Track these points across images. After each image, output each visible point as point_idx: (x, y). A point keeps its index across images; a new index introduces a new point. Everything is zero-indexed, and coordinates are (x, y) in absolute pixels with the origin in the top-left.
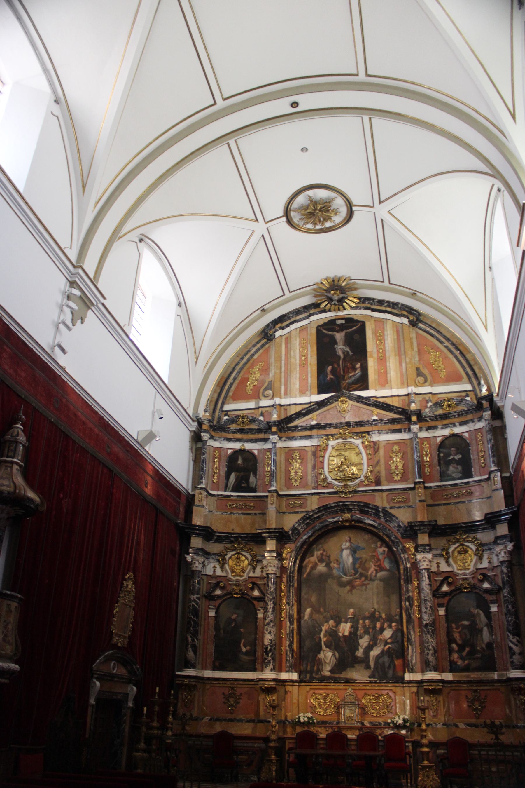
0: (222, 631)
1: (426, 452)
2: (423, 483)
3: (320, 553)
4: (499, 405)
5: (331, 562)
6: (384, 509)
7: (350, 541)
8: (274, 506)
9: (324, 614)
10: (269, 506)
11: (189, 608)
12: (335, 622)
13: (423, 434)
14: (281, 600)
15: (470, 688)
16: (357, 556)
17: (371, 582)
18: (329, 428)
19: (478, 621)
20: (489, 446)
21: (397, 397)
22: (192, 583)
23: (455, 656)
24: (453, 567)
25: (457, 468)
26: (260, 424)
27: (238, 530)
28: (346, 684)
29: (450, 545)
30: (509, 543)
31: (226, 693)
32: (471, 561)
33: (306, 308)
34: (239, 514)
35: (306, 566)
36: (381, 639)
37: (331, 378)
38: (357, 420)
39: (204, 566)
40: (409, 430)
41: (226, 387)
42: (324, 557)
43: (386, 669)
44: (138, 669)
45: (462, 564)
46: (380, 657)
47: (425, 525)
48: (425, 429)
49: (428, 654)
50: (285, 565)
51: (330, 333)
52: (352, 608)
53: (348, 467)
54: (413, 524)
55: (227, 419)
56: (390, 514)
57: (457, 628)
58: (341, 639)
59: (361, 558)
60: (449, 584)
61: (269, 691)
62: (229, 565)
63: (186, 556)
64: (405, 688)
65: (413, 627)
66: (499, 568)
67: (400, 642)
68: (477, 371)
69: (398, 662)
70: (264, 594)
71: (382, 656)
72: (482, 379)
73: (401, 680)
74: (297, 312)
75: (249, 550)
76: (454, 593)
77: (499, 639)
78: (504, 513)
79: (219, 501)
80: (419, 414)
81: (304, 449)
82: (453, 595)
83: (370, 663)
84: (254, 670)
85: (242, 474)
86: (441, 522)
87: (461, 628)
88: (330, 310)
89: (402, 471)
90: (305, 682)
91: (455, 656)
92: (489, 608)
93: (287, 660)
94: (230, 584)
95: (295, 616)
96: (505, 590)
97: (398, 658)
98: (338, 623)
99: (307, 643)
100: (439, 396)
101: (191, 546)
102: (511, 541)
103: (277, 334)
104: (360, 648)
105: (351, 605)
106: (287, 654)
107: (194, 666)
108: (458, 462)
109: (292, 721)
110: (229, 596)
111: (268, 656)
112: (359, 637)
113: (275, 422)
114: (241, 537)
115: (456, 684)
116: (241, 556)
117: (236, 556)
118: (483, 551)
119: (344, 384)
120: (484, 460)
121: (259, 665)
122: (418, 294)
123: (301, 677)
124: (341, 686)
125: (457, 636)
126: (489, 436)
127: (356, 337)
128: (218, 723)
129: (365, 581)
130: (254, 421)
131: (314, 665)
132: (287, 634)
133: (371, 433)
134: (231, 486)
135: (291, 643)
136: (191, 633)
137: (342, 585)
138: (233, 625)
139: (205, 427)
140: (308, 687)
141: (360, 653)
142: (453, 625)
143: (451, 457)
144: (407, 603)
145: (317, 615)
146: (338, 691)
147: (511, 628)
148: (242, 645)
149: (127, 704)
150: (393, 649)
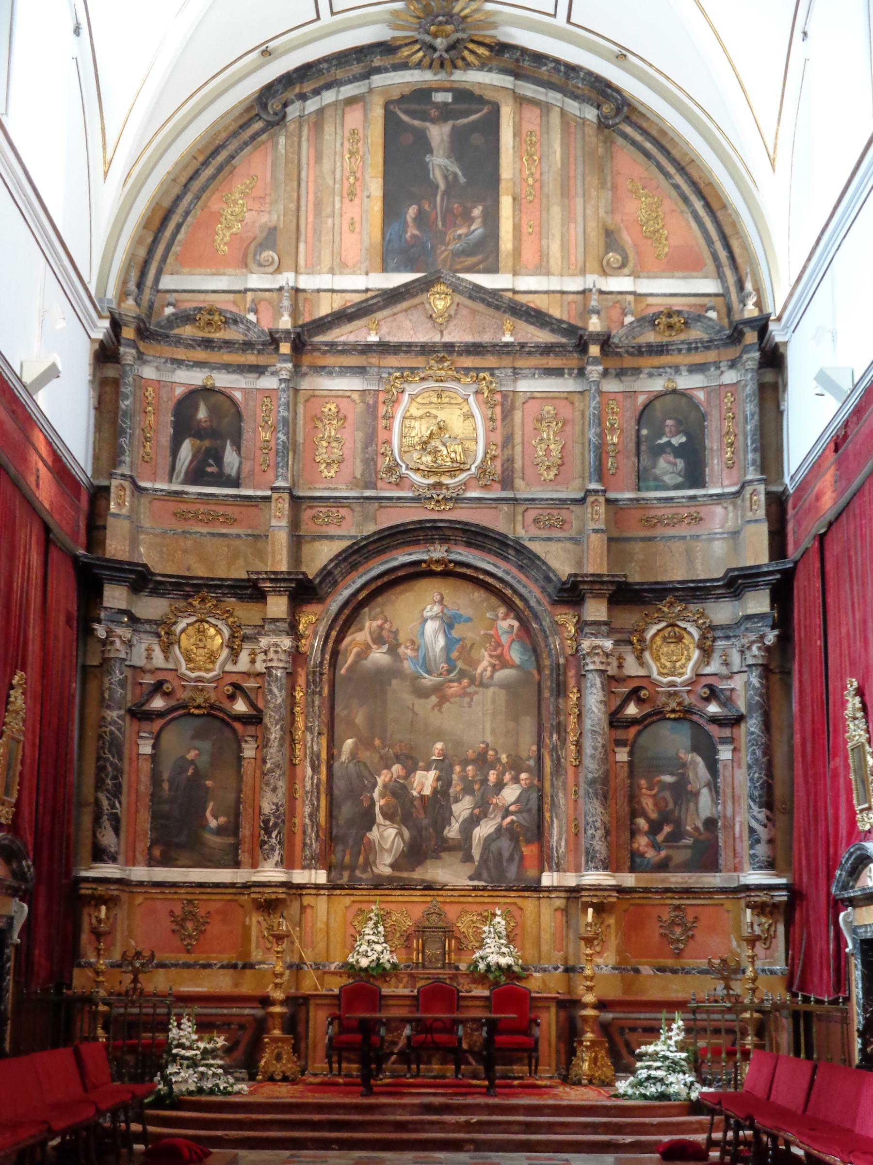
0: (166, 785)
1: (612, 425)
2: (604, 491)
3: (376, 623)
4: (778, 339)
5: (399, 645)
6: (517, 541)
7: (441, 602)
8: (284, 523)
9: (383, 752)
10: (274, 522)
11: (100, 737)
12: (404, 767)
13: (611, 386)
14: (293, 721)
15: (669, 902)
16: (455, 634)
17: (480, 690)
18: (406, 352)
19: (691, 775)
20: (749, 427)
21: (558, 295)
22: (107, 685)
23: (642, 842)
24: (649, 668)
25: (675, 464)
26: (248, 329)
27: (200, 571)
28: (426, 892)
29: (647, 624)
30: (768, 630)
31: (178, 912)
32: (689, 659)
33: (360, 53)
34: (202, 534)
35: (347, 651)
36: (496, 805)
37: (414, 236)
38: (469, 338)
39: (131, 646)
40: (581, 372)
41: (168, 233)
42: (385, 634)
43: (505, 864)
44: (29, 867)
45: (668, 664)
46: (494, 840)
47: (602, 583)
48: (613, 372)
49: (593, 836)
50: (303, 650)
51: (416, 123)
53: (445, 445)
54: (580, 579)
55: (173, 314)
56: (530, 551)
57: (650, 788)
58: (416, 803)
59: (462, 639)
60: (640, 701)
61: (270, 907)
62: (180, 647)
63: (96, 626)
64: (543, 901)
65: (565, 783)
66: (744, 676)
67: (535, 808)
68: (737, 251)
69: (529, 851)
70: (260, 711)
71: (498, 838)
72: (749, 276)
73: (536, 888)
74: (342, 58)
75: (223, 614)
76: (649, 720)
77: (729, 813)
78: (766, 569)
79: (156, 503)
80: (605, 341)
81: (349, 397)
82: (646, 723)
84: (237, 865)
85: (207, 443)
86: (635, 577)
87: (656, 789)
88: (419, 65)
89: (560, 462)
90: (342, 888)
91: (642, 842)
92: (715, 752)
93: (305, 844)
94: (184, 686)
95: (324, 755)
96: (754, 721)
97: (528, 842)
98: (410, 771)
99: (346, 811)
100: (650, 300)
101: (105, 604)
102: (773, 628)
103: (293, 111)
104: (453, 821)
105: (439, 735)
106: (304, 833)
107: (114, 859)
108: (679, 451)
109: (316, 964)
110: (181, 712)
111: (270, 837)
113: (287, 332)
114: (209, 587)
115: (641, 895)
116: (206, 626)
117: (197, 625)
118: (714, 640)
119: (443, 253)
120: (733, 453)
121: (246, 855)
122: (630, 57)
123: (333, 874)
124: (416, 896)
125: (648, 804)
126: (751, 408)
127: (476, 139)
128: (161, 971)
129: (470, 685)
130: (236, 322)
131: (359, 854)
132: (307, 793)
133: (497, 372)
134: (183, 471)
135: (316, 809)
136: (107, 790)
137: (422, 693)
138: (190, 772)
139: (128, 333)
140: (347, 898)
141: (453, 831)
142: (643, 782)
143: (664, 440)
144: (555, 736)
145: (368, 754)
146: (409, 906)
147: (756, 793)
148: (208, 814)
149: (11, 938)
150: (520, 825)
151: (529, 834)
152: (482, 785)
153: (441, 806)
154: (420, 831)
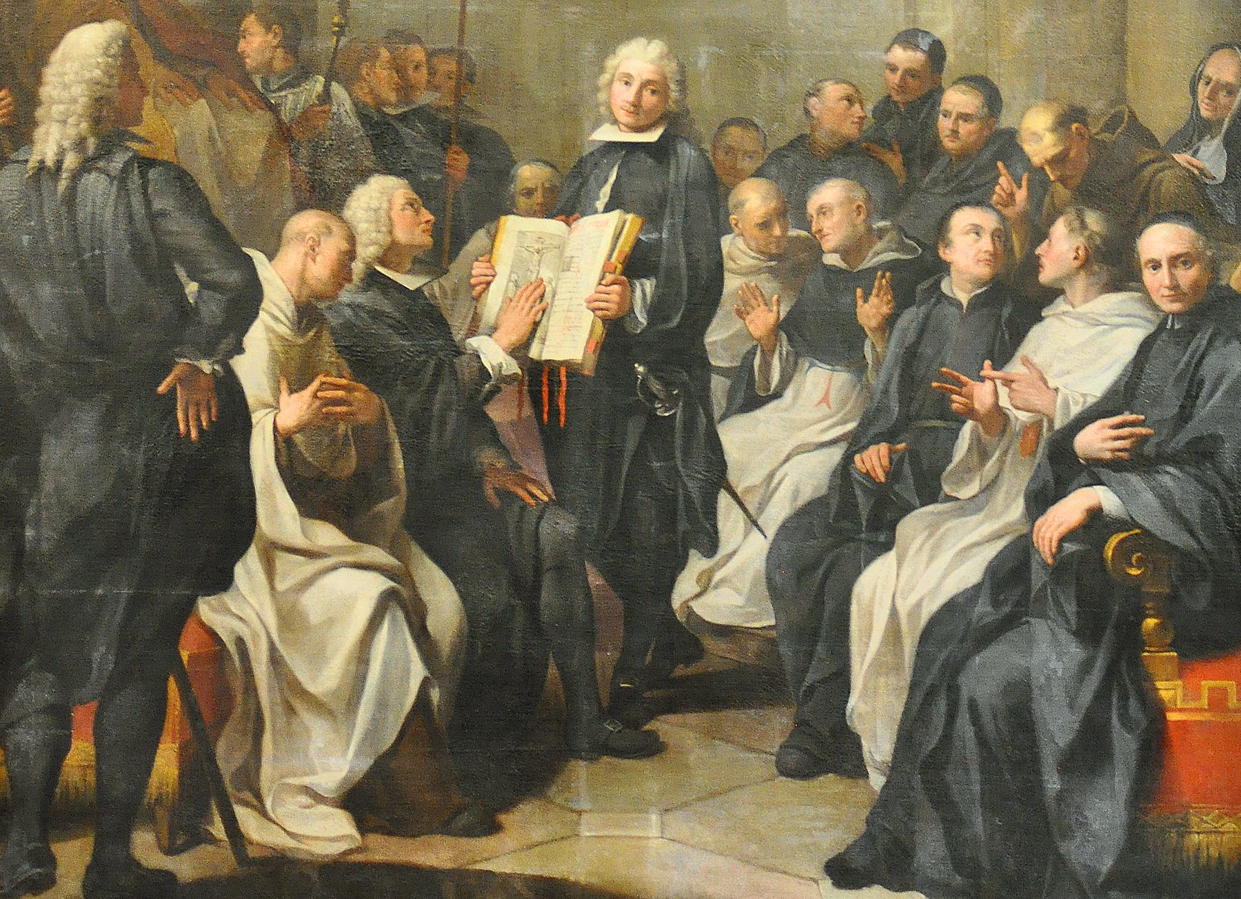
9: (292, 101)
12: (426, 194)
36: (997, 419)
43: (1053, 783)
46: (986, 636)
52: (649, 30)
58: (499, 413)
71: (1009, 623)
83: (853, 701)
104: (729, 518)
112: (719, 385)
145: (201, 109)
151: (1200, 598)
152: (903, 298)
153: (657, 429)
154: (527, 590)
